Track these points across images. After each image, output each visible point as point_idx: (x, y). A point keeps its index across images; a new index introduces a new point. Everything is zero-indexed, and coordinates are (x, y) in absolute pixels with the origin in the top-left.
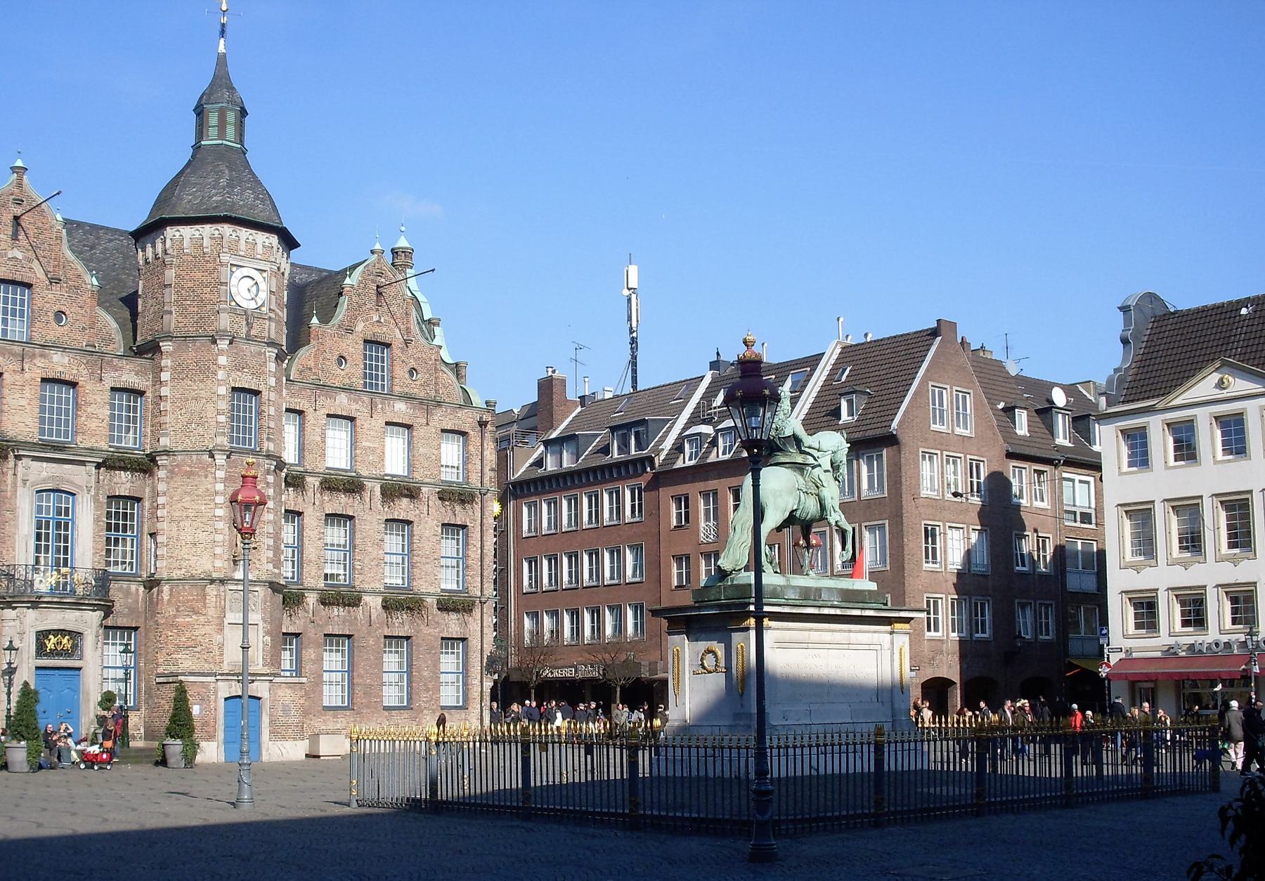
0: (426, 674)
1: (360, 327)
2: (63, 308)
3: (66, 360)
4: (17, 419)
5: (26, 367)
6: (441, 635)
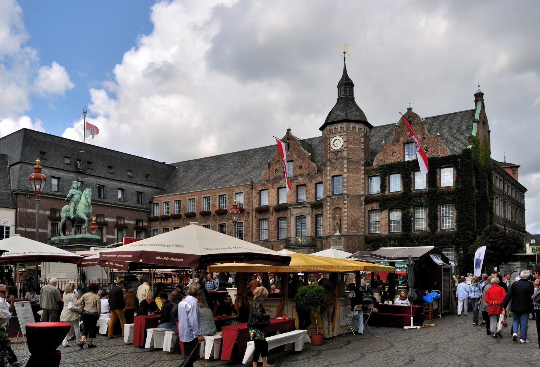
2: (301, 164)
3: (302, 179)
5: (292, 183)
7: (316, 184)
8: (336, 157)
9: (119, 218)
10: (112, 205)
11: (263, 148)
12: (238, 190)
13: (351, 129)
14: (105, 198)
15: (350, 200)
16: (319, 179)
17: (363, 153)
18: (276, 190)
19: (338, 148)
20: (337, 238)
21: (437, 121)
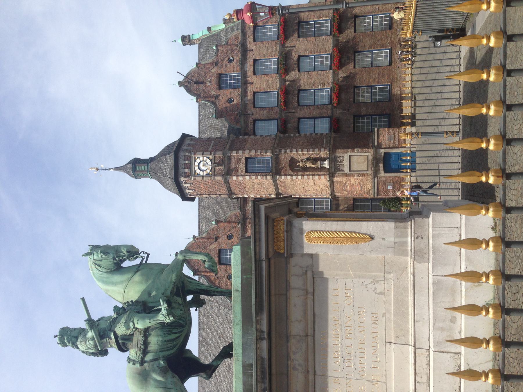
1: (213, 93)
11: (200, 330)
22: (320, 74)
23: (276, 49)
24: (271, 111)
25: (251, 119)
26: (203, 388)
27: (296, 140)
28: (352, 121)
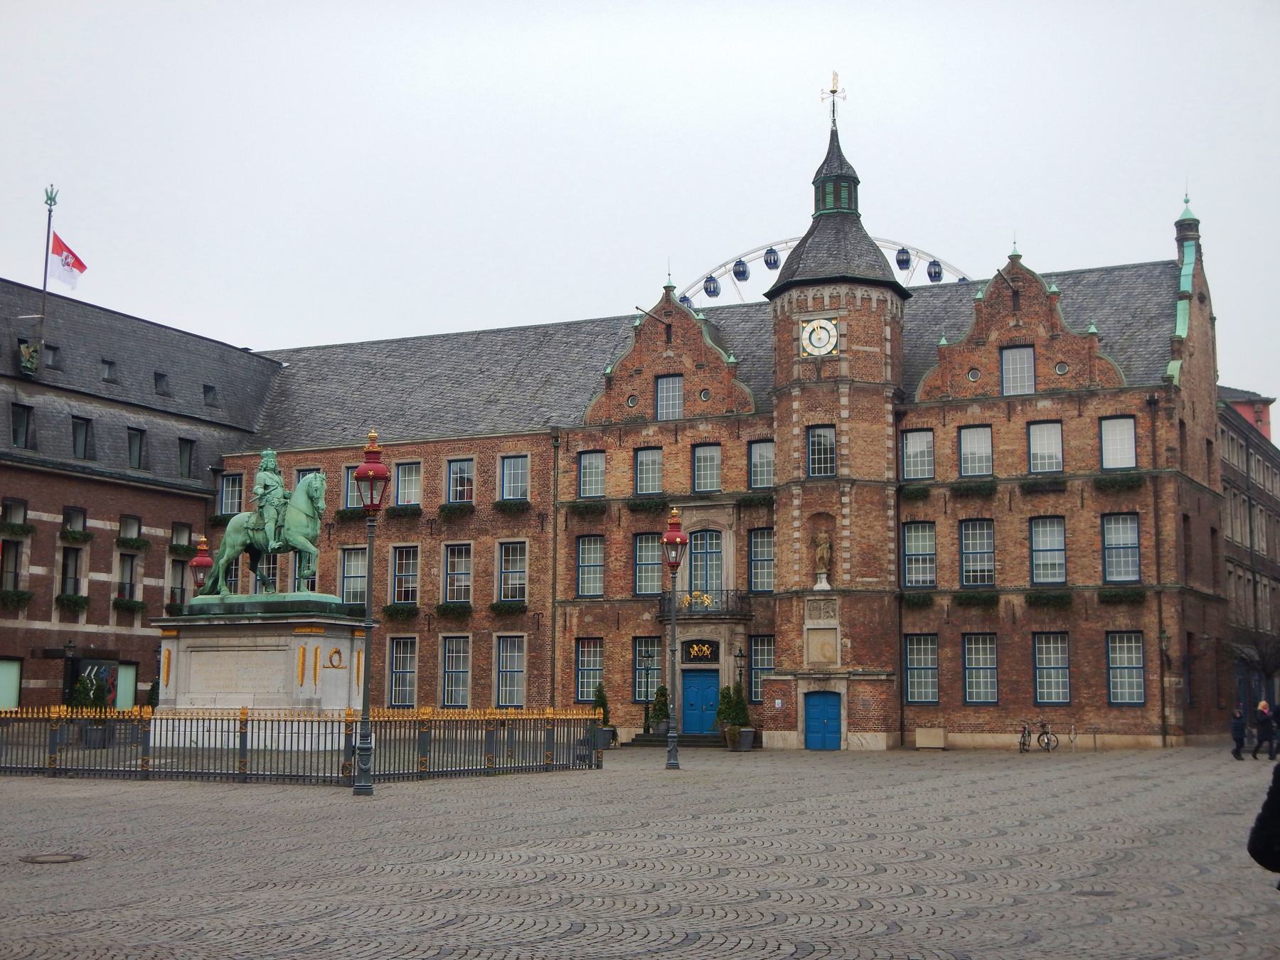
0: (1087, 669)
1: (994, 336)
2: (707, 387)
3: (710, 426)
4: (674, 479)
5: (679, 438)
6: (1106, 629)
7: (750, 443)
8: (819, 375)
9: (69, 513)
10: (112, 480)
12: (509, 448)
13: (859, 303)
14: (93, 458)
15: (856, 493)
16: (761, 431)
17: (889, 368)
18: (631, 453)
19: (824, 352)
20: (822, 598)
21: (1076, 284)
22: (1022, 563)
23: (1080, 468)
24: (950, 465)
25: (935, 422)
26: (465, 344)
27: (876, 523)
28: (925, 630)
